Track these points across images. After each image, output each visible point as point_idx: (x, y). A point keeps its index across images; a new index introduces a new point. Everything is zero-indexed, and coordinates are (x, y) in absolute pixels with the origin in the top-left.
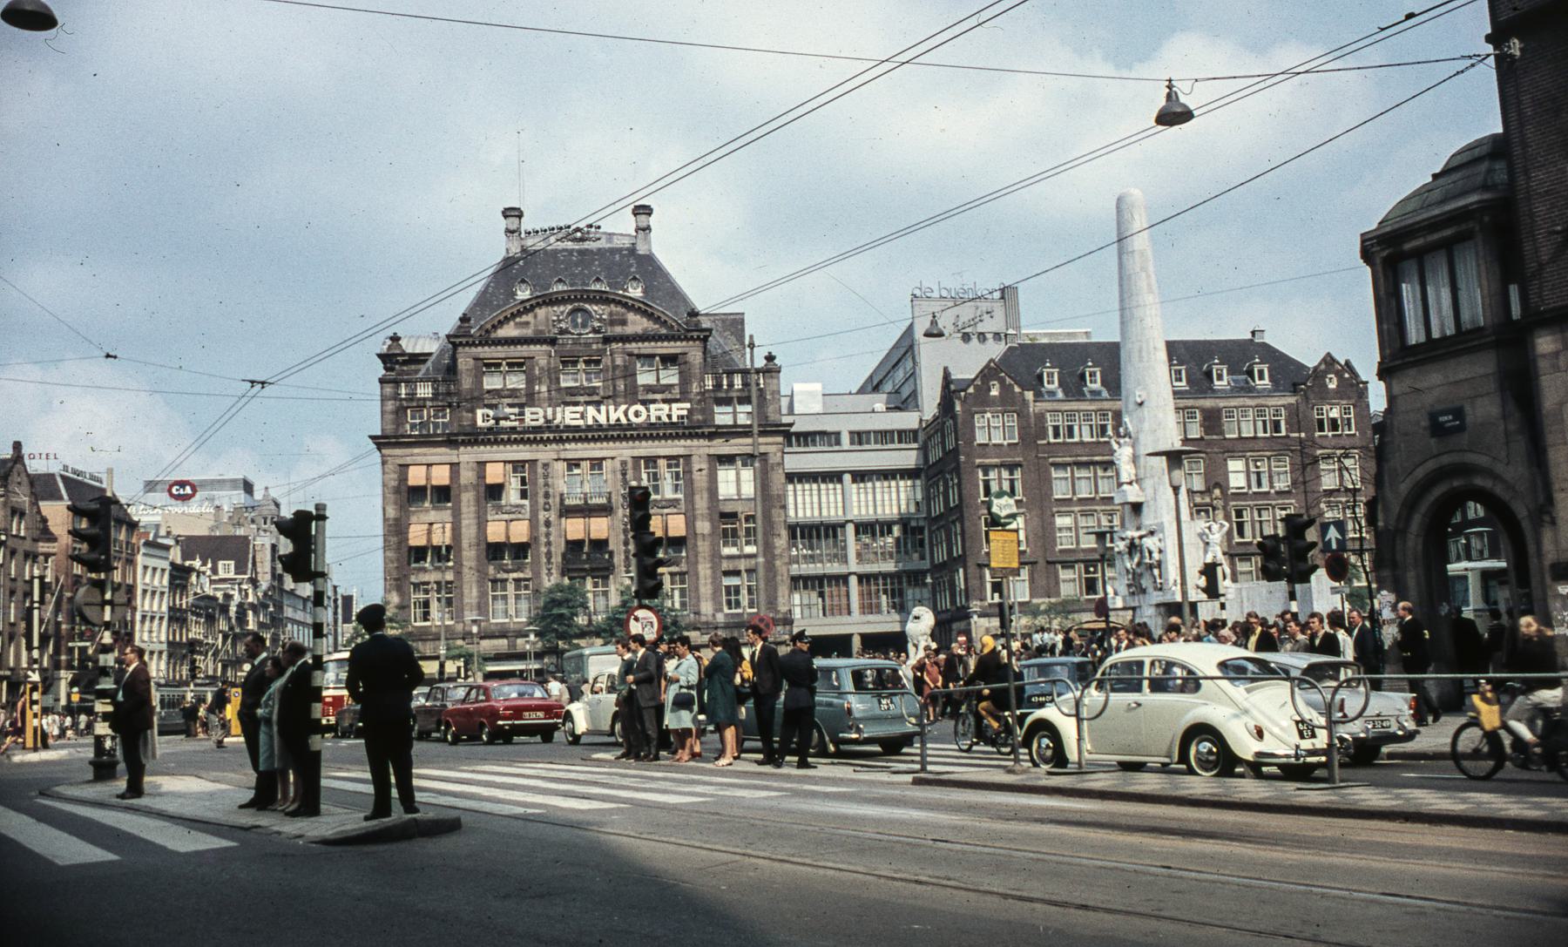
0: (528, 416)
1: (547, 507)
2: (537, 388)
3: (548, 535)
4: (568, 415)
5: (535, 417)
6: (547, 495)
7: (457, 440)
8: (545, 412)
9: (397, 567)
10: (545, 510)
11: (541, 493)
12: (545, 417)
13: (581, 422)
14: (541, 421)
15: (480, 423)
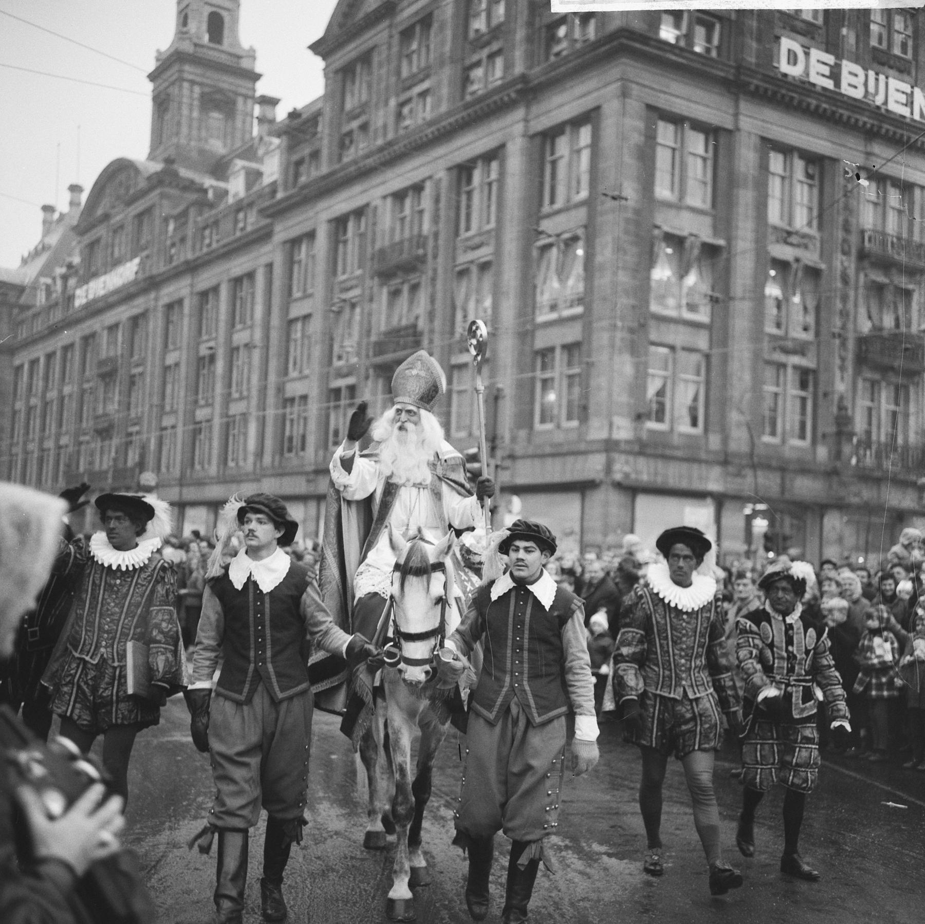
0: (846, 79)
1: (846, 248)
2: (844, 31)
3: (845, 299)
4: (894, 96)
5: (853, 80)
6: (847, 228)
7: (749, 83)
8: (867, 76)
9: (633, 307)
10: (844, 253)
11: (841, 219)
12: (866, 84)
13: (905, 111)
14: (858, 94)
15: (784, 67)
